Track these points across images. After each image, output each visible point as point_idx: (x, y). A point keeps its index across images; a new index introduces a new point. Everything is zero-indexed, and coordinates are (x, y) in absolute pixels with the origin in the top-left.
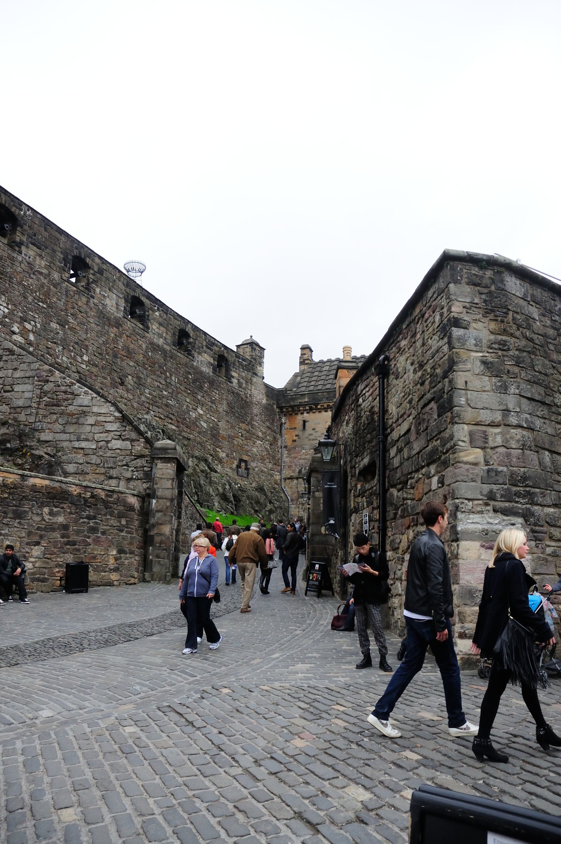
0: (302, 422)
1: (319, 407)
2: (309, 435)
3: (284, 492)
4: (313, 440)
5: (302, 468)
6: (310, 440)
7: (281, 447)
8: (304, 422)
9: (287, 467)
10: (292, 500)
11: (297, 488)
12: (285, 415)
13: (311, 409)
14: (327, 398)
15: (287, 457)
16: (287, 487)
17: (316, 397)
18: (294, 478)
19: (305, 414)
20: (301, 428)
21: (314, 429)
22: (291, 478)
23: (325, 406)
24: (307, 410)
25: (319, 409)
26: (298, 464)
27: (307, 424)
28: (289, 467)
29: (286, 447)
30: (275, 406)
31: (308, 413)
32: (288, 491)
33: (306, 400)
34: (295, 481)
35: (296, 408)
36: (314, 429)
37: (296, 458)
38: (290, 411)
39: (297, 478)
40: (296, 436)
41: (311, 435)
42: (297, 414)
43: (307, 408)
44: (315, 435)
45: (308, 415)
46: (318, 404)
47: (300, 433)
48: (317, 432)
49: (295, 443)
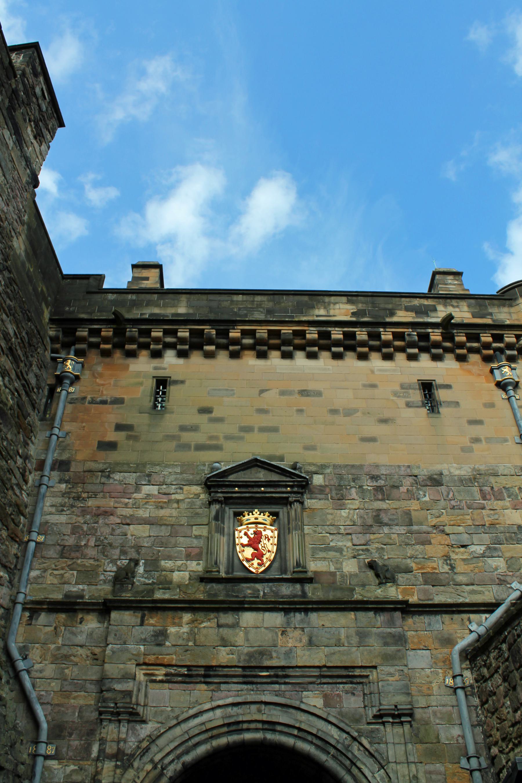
0: (150, 384)
1: (234, 334)
2: (183, 428)
3: (17, 676)
4: (200, 447)
5: (137, 563)
6: (185, 447)
7: (41, 465)
8: (162, 383)
9: (52, 553)
10: (58, 731)
11: (98, 659)
12: (79, 353)
13: (196, 344)
14: (269, 312)
15: (60, 509)
16: (35, 653)
17: (226, 304)
18: (89, 608)
19: (170, 358)
20: (148, 403)
21: (205, 410)
22: (70, 607)
23: (262, 332)
24: (182, 341)
25: (236, 342)
26: (117, 540)
27: (173, 390)
28: (65, 552)
29: (62, 465)
30: (47, 315)
31: (182, 354)
32: (41, 674)
33: (182, 310)
34: (91, 624)
35: (132, 331)
36: (205, 410)
37: (107, 514)
38: (106, 340)
39: (105, 609)
40: (119, 427)
41: (194, 428)
42: (132, 354)
43: (184, 333)
44: (207, 429)
45: (181, 361)
46: (234, 323)
47: (140, 420)
48: (220, 420)
49: (113, 457)
